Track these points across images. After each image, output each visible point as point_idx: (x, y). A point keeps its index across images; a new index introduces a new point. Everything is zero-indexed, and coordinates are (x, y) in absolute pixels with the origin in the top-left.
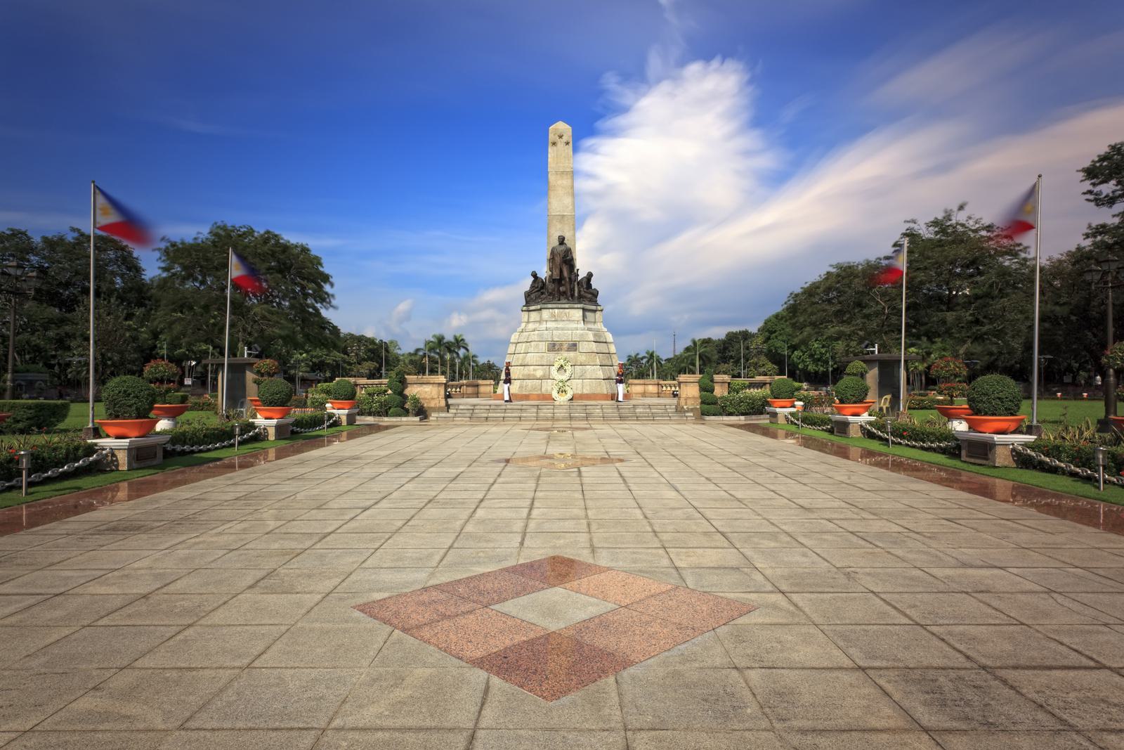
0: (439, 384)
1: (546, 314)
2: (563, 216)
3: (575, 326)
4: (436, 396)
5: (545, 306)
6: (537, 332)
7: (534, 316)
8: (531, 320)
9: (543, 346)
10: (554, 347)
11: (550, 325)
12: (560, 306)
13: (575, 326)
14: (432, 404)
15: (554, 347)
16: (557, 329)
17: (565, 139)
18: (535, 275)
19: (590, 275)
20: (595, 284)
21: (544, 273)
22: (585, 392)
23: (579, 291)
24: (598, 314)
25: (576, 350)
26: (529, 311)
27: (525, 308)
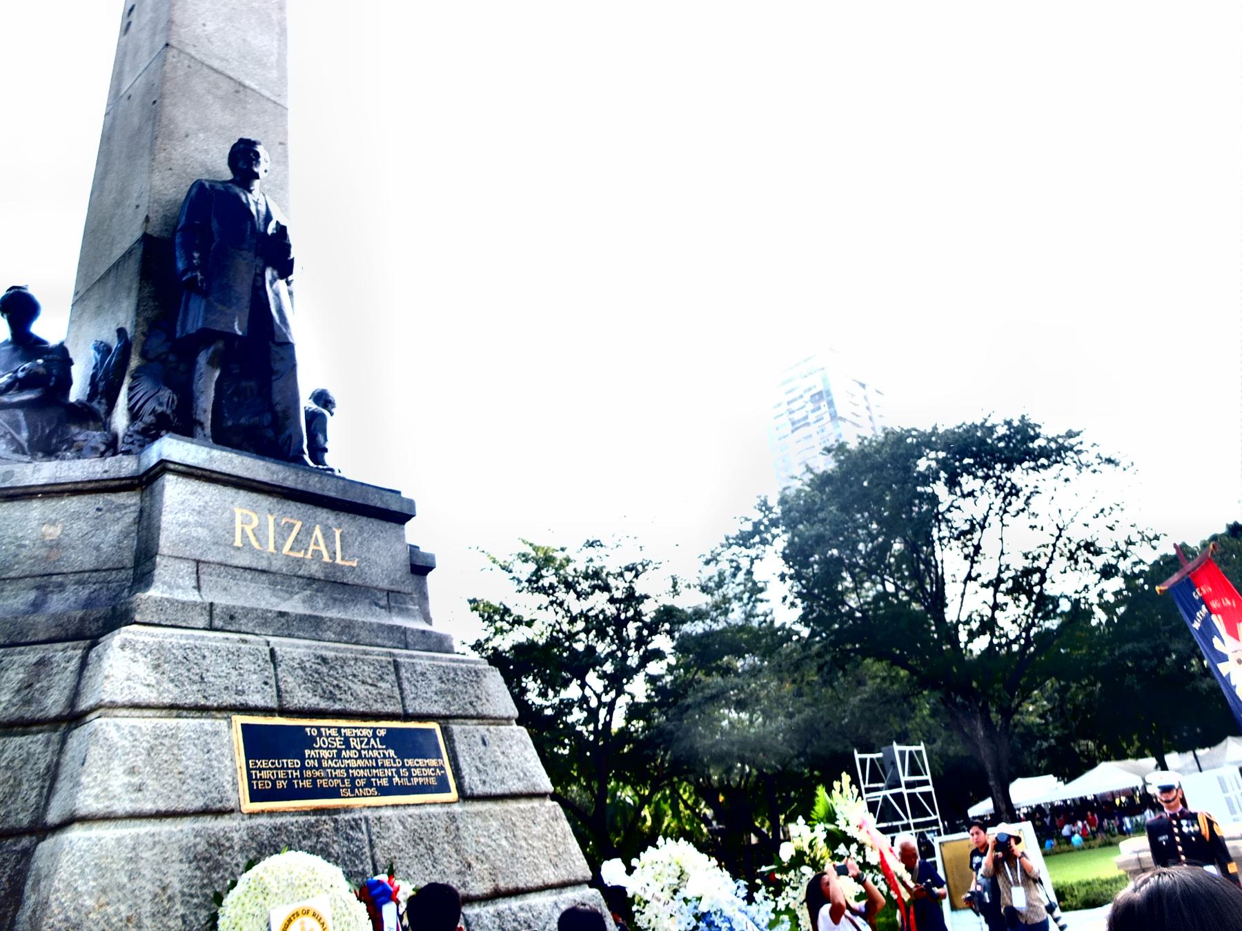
25: (442, 787)
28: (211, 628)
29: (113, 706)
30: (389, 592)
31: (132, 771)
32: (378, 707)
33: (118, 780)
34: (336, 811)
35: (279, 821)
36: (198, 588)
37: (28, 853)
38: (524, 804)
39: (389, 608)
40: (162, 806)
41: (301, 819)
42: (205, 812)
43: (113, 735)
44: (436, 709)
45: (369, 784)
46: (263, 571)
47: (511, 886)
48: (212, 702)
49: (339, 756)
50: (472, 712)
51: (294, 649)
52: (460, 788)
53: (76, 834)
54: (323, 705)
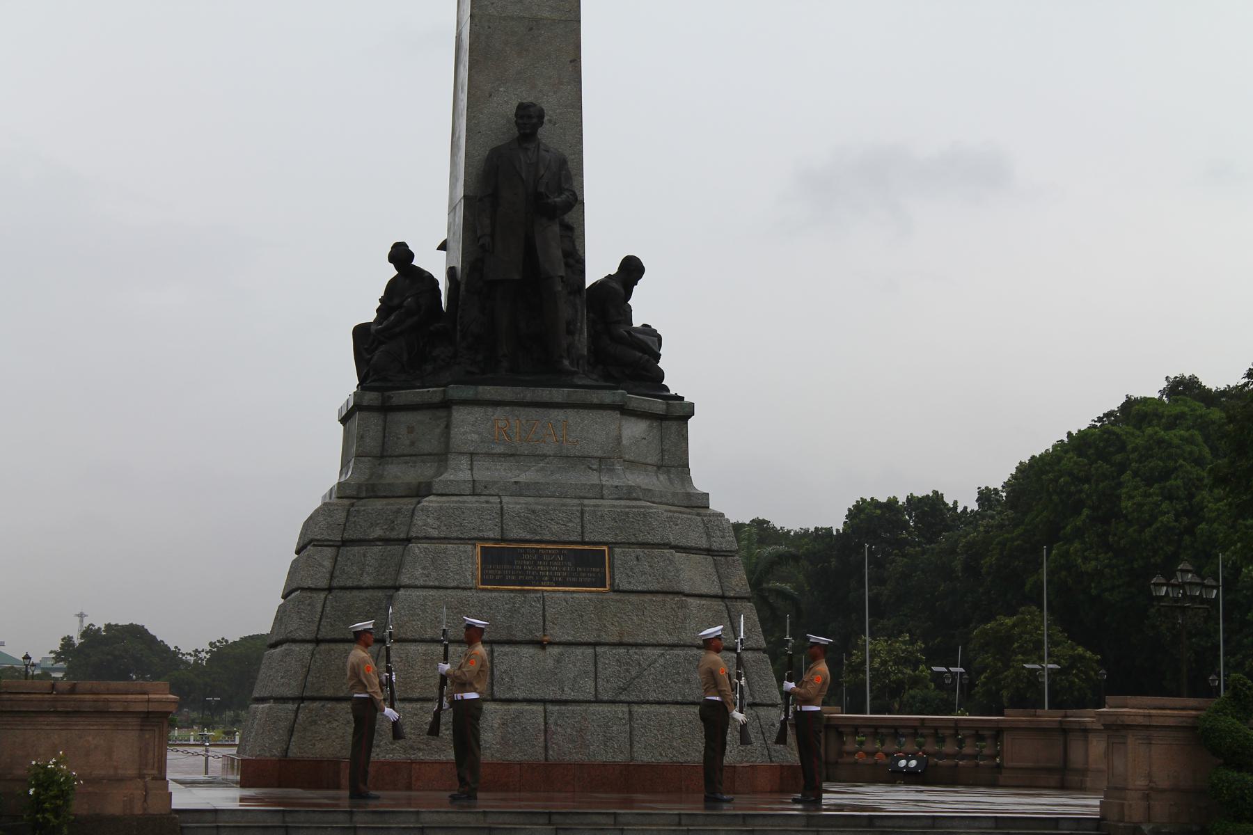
1: (469, 425)
3: (593, 478)
4: (131, 772)
5: (468, 392)
6: (430, 502)
11: (487, 472)
12: (529, 394)
13: (593, 478)
16: (519, 489)
19: (631, 270)
20: (643, 307)
22: (643, 757)
23: (594, 337)
24: (674, 425)
26: (385, 409)
27: (371, 398)
28: (474, 494)
29: (417, 538)
30: (601, 459)
31: (424, 568)
32: (565, 538)
33: (418, 572)
34: (529, 591)
35: (494, 594)
36: (471, 469)
37: (391, 597)
38: (660, 598)
39: (599, 470)
40: (437, 584)
41: (506, 595)
42: (457, 588)
43: (417, 551)
44: (606, 539)
45: (551, 580)
46: (512, 455)
47: (631, 641)
48: (465, 536)
49: (535, 564)
50: (633, 540)
51: (513, 504)
52: (612, 585)
53: (402, 592)
54: (528, 537)
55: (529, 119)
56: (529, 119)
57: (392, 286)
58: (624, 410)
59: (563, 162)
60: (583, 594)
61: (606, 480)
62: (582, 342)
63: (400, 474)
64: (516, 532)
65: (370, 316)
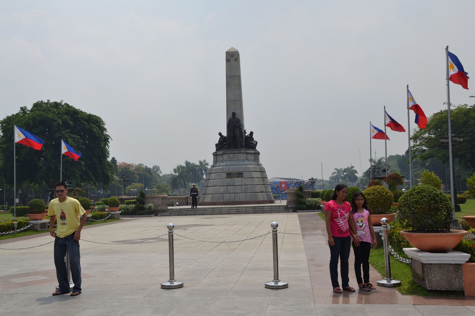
0: (163, 198)
2: (235, 101)
7: (220, 158)
8: (218, 160)
9: (224, 175)
10: (229, 175)
12: (233, 152)
14: (159, 208)
15: (229, 175)
16: (232, 165)
17: (234, 58)
18: (220, 134)
19: (252, 133)
20: (255, 137)
21: (225, 134)
22: (248, 200)
55: (234, 114)
56: (234, 114)
57: (220, 139)
58: (247, 153)
59: (239, 120)
60: (240, 179)
61: (244, 163)
62: (244, 144)
63: (218, 164)
64: (231, 171)
65: (217, 142)
